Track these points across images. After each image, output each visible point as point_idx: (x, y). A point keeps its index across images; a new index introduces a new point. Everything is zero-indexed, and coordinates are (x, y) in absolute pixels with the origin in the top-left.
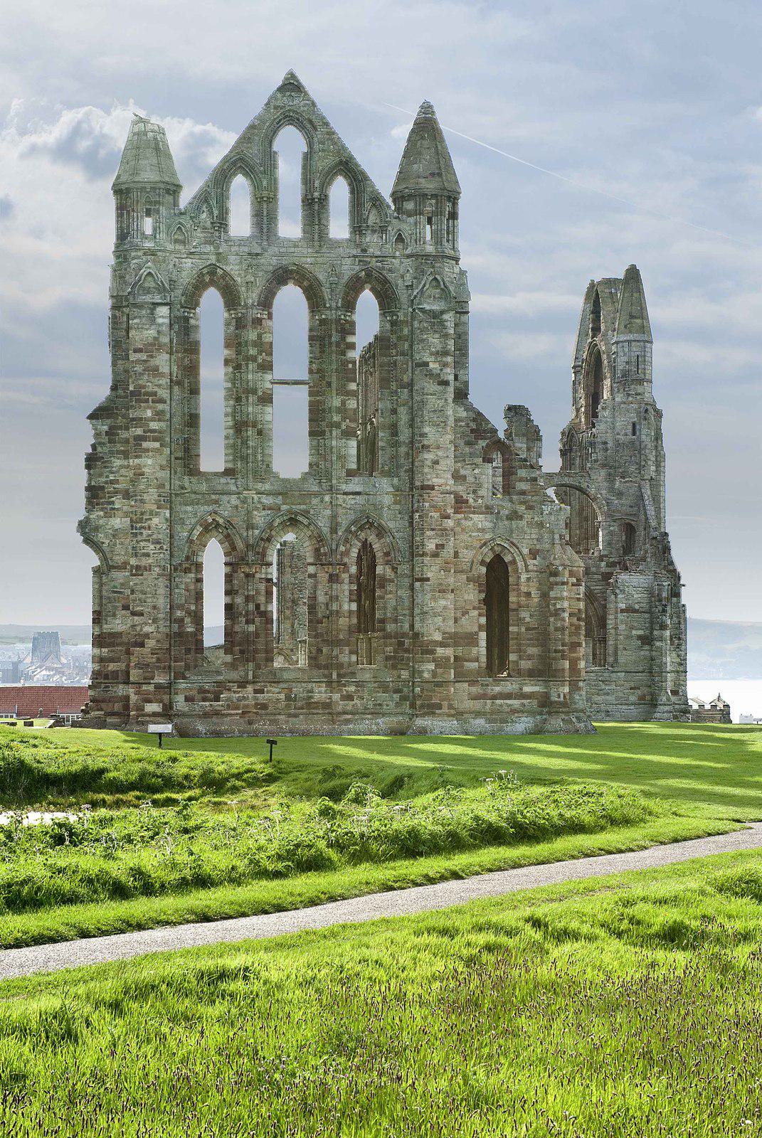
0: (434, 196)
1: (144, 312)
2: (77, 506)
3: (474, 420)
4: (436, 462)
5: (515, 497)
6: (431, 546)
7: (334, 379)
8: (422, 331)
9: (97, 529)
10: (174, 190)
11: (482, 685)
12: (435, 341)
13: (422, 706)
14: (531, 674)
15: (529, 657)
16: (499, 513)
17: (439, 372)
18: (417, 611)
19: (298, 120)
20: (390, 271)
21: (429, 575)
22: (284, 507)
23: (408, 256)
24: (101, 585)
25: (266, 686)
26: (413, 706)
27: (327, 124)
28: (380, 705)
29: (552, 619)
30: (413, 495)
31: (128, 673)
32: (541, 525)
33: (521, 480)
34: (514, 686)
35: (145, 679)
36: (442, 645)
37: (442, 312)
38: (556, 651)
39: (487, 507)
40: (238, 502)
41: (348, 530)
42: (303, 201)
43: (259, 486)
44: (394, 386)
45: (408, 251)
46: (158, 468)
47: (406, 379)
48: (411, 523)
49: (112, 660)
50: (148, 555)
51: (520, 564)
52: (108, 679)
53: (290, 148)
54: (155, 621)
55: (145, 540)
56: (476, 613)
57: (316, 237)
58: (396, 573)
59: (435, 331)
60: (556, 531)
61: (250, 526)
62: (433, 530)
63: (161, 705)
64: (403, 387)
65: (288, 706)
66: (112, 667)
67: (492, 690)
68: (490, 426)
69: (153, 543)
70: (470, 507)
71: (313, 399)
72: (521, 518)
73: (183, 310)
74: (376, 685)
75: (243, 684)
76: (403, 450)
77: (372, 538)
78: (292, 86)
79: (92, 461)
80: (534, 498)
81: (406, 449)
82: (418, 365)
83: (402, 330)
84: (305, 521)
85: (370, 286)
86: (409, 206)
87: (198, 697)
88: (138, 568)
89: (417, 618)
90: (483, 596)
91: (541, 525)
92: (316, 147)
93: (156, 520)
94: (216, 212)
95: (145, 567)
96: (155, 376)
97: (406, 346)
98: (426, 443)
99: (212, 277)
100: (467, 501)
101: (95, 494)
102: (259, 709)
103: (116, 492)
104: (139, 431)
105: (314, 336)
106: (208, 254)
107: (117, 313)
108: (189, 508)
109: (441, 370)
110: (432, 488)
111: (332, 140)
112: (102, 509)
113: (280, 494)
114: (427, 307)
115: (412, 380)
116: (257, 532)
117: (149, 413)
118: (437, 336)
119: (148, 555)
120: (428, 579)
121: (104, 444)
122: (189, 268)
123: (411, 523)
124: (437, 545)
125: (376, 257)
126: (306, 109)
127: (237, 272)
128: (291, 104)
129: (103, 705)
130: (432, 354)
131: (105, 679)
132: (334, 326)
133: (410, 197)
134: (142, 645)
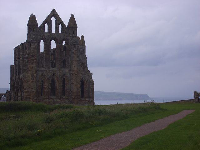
10: (37, 25)
12: (75, 49)
21: (73, 83)
31: (30, 97)
32: (88, 76)
51: (86, 81)
53: (53, 19)
56: (79, 88)
61: (48, 75)
72: (86, 75)
76: (69, 65)
77: (65, 78)
78: (54, 11)
91: (88, 76)
92: (58, 20)
104: (33, 61)
110: (74, 70)
117: (34, 58)
123: (71, 75)
128: (54, 13)
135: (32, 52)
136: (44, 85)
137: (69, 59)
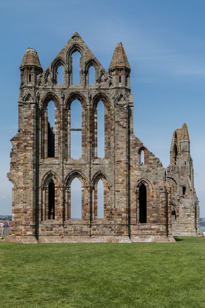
0: (122, 69)
2: (7, 168)
3: (135, 140)
4: (122, 153)
5: (149, 165)
6: (121, 180)
7: (89, 128)
8: (118, 111)
9: (13, 176)
11: (138, 226)
13: (117, 233)
14: (154, 222)
15: (153, 217)
16: (143, 170)
17: (123, 124)
18: (116, 202)
19: (78, 47)
20: (107, 93)
21: (120, 190)
22: (73, 169)
23: (113, 89)
24: (15, 193)
25: (67, 226)
26: (115, 232)
27: (88, 48)
28: (104, 232)
29: (160, 204)
30: (115, 165)
32: (157, 174)
33: (150, 159)
34: (148, 226)
35: (27, 224)
36: (124, 212)
37: (124, 105)
38: (162, 215)
39: (139, 168)
40: (58, 167)
41: (94, 176)
42: (80, 73)
43: (65, 162)
44: (109, 130)
46: (31, 155)
47: (113, 127)
48: (114, 173)
49: (18, 218)
50: (28, 184)
51: (150, 187)
52: (17, 224)
54: (30, 205)
55: (27, 179)
57: (84, 83)
58: (110, 190)
60: (162, 176)
62: (121, 175)
63: (32, 232)
64: (111, 130)
65: (75, 233)
66: (18, 220)
67: (141, 227)
68: (140, 142)
69: (30, 180)
70: (134, 168)
71: (83, 134)
72: (150, 172)
73: (41, 106)
74: (103, 226)
75: (60, 225)
76: (112, 150)
79: (12, 154)
80: (154, 165)
81: (113, 150)
82: (116, 122)
83: (111, 112)
84: (81, 173)
85: (101, 99)
86: (114, 73)
87: (45, 229)
88: (25, 188)
89: (116, 204)
90: (138, 197)
93: (31, 172)
94: (52, 76)
95: (27, 188)
96: (31, 126)
97: (113, 117)
98: (118, 147)
99: (50, 97)
100: (132, 167)
101: (13, 165)
102: (65, 233)
103: (20, 164)
106: (49, 89)
107: (21, 108)
108: (43, 169)
109: (124, 123)
111: (89, 53)
112: (15, 170)
113: (72, 164)
114: (119, 104)
115: (114, 127)
116: (65, 177)
117: (29, 138)
118: (122, 112)
119: (28, 184)
120: (119, 191)
121: (16, 149)
122: (43, 94)
123: (114, 173)
124: (122, 180)
125: (103, 89)
126: (81, 43)
127: (58, 94)
129: (15, 232)
130: (121, 119)
131: (15, 224)
132: (89, 111)
133: (113, 71)
134: (26, 213)
135: (25, 124)
136: (56, 196)
137: (112, 138)
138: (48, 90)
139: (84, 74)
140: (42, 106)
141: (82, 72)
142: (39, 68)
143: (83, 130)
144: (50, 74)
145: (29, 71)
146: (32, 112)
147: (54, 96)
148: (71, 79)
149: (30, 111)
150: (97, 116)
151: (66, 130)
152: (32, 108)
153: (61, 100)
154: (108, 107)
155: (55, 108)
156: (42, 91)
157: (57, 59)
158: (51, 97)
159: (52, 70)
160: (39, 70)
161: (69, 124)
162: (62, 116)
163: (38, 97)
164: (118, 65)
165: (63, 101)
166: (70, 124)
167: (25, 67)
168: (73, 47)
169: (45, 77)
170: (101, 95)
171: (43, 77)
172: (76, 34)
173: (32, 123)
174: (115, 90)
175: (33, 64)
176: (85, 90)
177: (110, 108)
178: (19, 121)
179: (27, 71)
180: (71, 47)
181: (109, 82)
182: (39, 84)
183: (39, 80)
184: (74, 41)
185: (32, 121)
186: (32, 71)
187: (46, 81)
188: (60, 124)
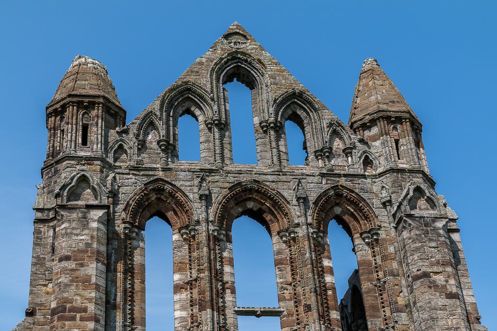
1: (74, 215)
17: (444, 283)
19: (246, 61)
37: (435, 219)
45: (380, 170)
47: (401, 301)
59: (431, 240)
73: (123, 225)
82: (416, 278)
94: (163, 133)
105: (281, 259)
106: (154, 169)
107: (43, 228)
109: (447, 281)
111: (283, 76)
118: (433, 244)
126: (253, 51)
127: (188, 188)
135: (64, 279)
138: (151, 173)
139: (272, 132)
140: (127, 225)
141: (266, 126)
142: (117, 110)
143: (285, 313)
144: (156, 129)
145: (81, 112)
146: (92, 237)
147: (171, 195)
148: (226, 146)
149: (82, 233)
150: (331, 265)
151: (221, 311)
152: (95, 225)
153: (198, 211)
154: (369, 232)
155: (176, 237)
156: (129, 177)
157: (178, 87)
158: (158, 199)
159: (161, 114)
160: (115, 115)
161: (228, 291)
162: (205, 259)
163: (114, 195)
164: (385, 107)
165: (207, 208)
166: (233, 292)
167: (68, 99)
168: (228, 60)
169: (137, 136)
170: (339, 195)
171: (131, 135)
172: (237, 29)
173: (90, 276)
174: (388, 180)
175: (97, 93)
176: (284, 178)
177: (377, 234)
178: (33, 274)
179: (77, 112)
180: (222, 59)
181: (360, 158)
182: (117, 156)
183: (117, 141)
184: (232, 44)
185: (92, 269)
186: (94, 113)
187: (142, 146)
188: (195, 291)
